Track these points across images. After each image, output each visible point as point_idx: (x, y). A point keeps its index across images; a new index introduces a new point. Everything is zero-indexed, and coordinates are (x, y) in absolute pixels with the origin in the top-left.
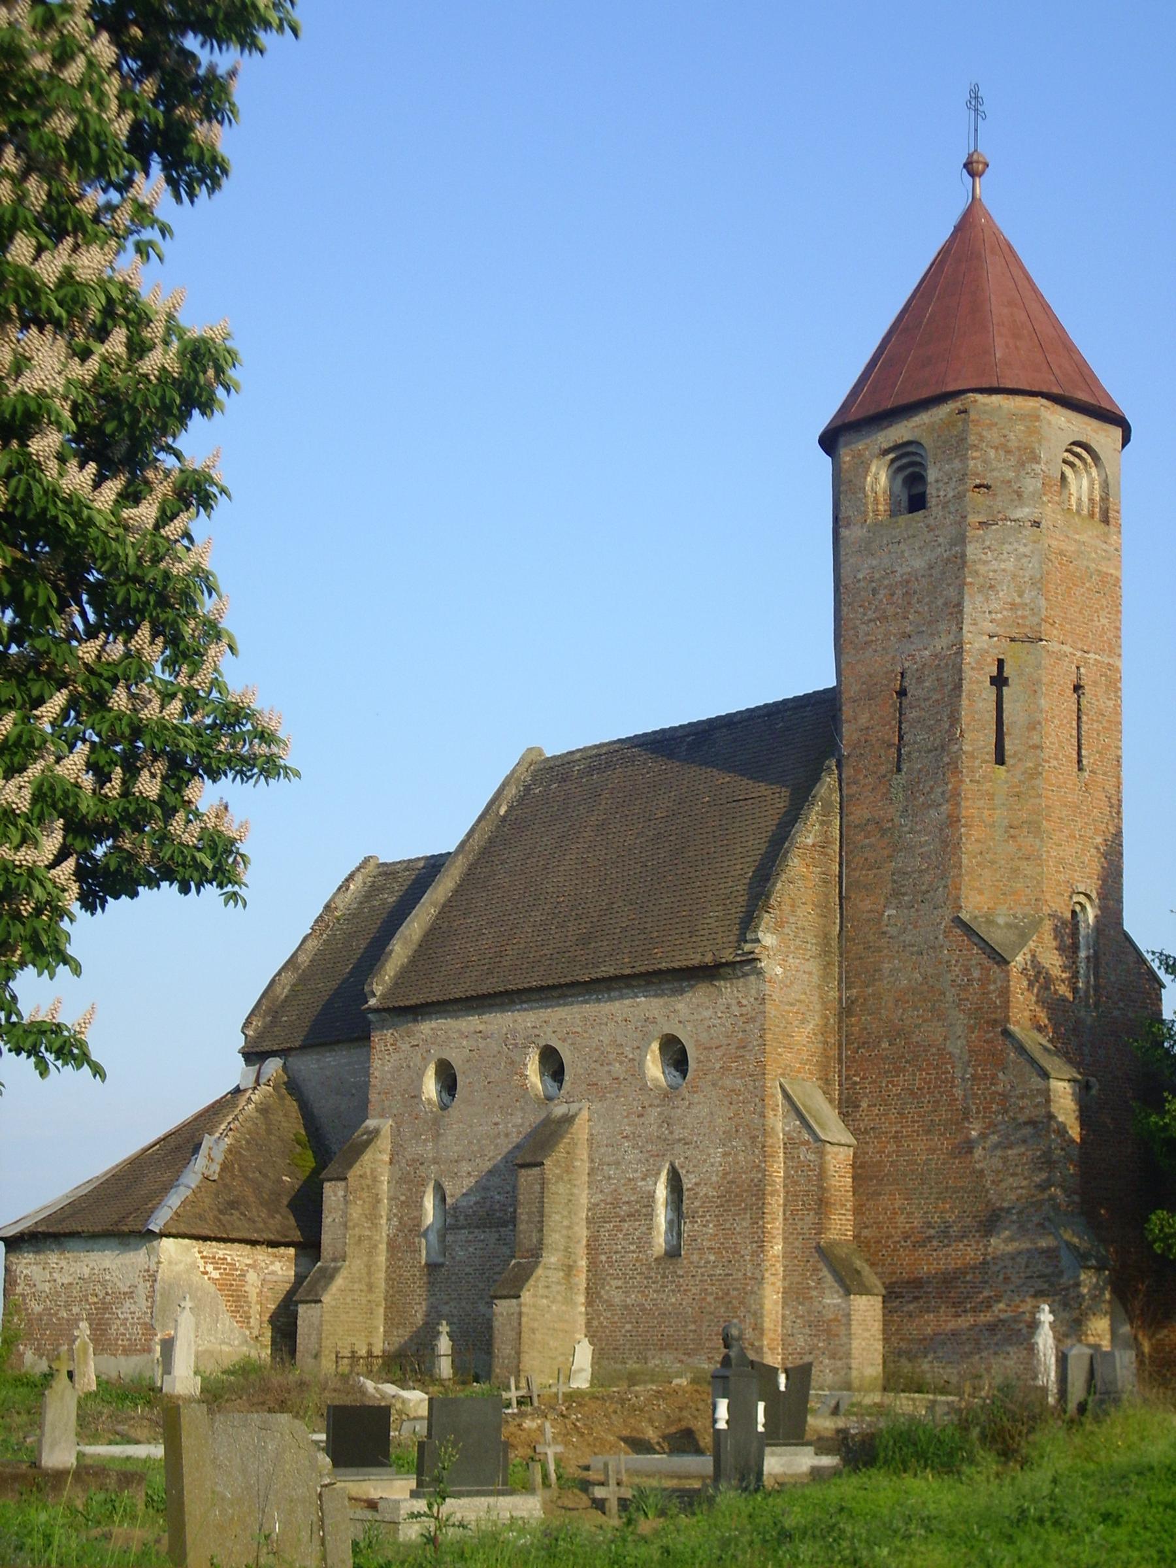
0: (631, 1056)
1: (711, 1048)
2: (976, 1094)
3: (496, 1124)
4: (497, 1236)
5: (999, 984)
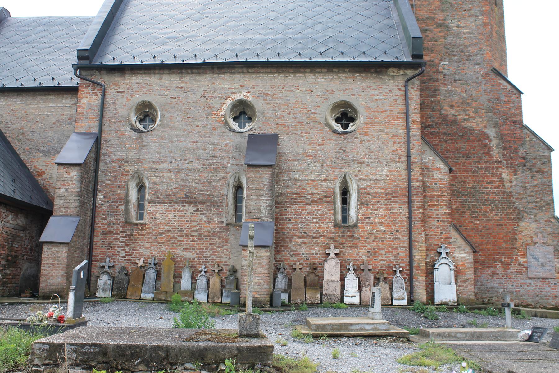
0: (313, 111)
1: (379, 112)
2: (506, 155)
3: (197, 142)
4: (195, 209)
5: (516, 104)
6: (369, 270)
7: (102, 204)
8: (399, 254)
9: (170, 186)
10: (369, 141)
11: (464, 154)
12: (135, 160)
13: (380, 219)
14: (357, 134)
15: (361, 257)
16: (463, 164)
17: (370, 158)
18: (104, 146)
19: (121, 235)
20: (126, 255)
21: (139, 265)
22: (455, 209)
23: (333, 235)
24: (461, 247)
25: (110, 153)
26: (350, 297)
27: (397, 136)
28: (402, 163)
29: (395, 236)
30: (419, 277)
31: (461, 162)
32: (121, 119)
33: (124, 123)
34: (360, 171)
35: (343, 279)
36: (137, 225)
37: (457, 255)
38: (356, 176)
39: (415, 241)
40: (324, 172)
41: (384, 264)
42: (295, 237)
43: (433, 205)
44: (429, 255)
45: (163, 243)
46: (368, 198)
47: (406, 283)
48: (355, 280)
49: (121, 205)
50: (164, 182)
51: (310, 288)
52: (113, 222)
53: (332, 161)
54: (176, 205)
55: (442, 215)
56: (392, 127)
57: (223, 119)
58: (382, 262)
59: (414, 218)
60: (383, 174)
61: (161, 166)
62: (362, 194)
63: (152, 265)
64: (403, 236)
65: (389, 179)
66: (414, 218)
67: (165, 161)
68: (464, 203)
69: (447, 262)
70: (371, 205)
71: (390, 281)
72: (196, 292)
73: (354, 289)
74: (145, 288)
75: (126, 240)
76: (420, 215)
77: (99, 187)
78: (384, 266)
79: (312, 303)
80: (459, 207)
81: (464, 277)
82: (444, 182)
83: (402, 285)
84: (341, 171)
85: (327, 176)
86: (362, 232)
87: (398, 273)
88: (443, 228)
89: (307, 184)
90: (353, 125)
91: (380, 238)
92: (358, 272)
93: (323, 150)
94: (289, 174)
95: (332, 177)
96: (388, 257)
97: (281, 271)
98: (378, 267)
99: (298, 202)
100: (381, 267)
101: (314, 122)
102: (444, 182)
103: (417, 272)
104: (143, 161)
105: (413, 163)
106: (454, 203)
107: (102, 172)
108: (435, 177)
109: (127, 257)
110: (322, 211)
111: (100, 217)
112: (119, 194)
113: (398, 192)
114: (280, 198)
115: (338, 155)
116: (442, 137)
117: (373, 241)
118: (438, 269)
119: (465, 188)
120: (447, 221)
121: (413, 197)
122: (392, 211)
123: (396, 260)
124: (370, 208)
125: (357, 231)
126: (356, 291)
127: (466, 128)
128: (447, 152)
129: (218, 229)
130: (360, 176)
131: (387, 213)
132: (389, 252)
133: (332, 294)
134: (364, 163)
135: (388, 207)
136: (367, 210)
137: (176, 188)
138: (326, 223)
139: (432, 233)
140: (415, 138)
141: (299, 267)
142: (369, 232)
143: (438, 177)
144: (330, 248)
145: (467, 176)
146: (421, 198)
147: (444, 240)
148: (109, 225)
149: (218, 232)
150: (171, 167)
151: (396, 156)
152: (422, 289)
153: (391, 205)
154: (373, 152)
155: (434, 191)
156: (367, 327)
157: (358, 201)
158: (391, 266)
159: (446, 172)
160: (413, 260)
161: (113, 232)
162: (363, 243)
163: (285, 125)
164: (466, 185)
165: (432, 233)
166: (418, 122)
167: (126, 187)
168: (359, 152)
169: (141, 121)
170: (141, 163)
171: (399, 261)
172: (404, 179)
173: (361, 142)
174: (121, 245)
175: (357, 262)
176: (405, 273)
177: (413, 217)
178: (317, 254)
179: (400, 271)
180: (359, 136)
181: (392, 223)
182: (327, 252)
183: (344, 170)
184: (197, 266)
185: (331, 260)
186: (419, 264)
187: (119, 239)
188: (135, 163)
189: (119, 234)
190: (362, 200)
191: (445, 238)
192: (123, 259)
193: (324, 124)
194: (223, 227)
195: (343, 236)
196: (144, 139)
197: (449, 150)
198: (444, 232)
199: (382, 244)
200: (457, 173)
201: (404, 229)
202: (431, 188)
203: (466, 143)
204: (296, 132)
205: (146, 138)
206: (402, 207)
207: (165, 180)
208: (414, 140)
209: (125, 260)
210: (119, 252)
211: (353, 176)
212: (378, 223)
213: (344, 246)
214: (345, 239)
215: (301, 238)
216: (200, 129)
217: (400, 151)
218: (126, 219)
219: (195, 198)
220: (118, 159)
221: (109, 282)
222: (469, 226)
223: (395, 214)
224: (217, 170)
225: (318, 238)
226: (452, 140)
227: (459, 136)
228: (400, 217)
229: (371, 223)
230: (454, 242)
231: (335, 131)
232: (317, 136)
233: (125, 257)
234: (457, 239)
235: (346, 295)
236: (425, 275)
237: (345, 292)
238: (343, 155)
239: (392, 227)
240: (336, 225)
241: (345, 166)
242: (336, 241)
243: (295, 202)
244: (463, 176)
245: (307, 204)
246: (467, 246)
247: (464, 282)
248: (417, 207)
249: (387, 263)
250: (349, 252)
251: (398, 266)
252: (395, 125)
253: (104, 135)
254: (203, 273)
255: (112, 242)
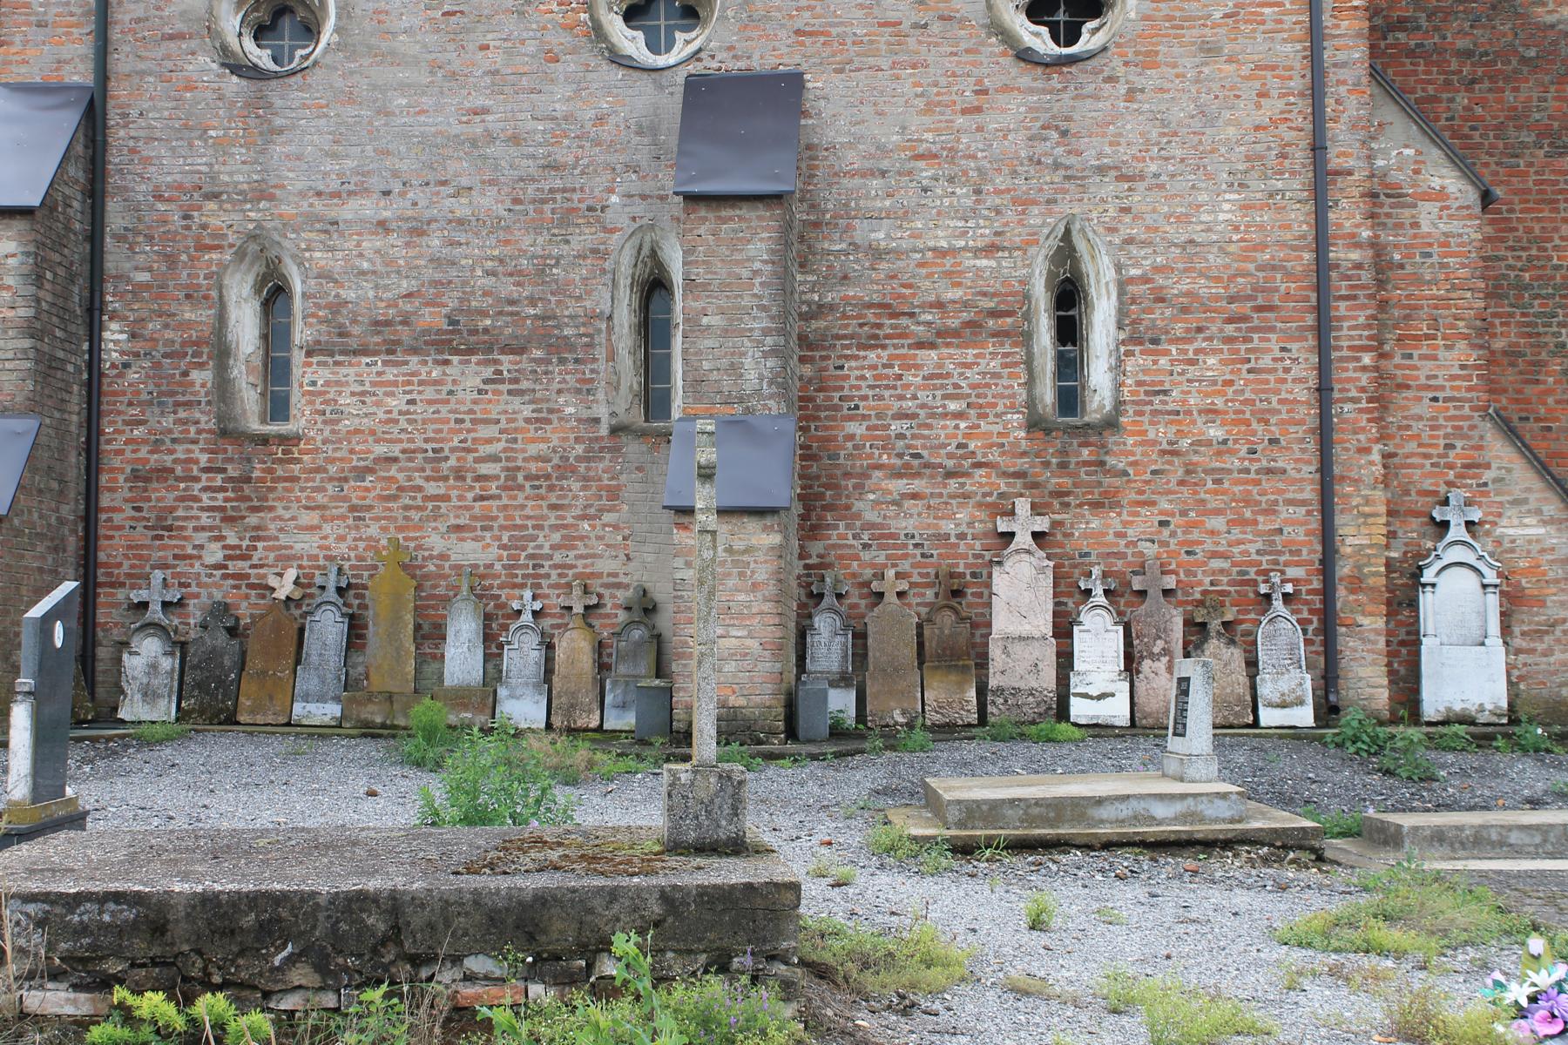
3: (485, 111)
4: (488, 372)
6: (1167, 593)
7: (126, 365)
8: (1280, 531)
9: (386, 288)
10: (1162, 90)
11: (1544, 133)
12: (245, 186)
13: (1207, 395)
14: (1115, 64)
15: (1134, 544)
16: (1537, 173)
17: (1167, 159)
18: (119, 136)
19: (203, 483)
20: (227, 557)
21: (281, 594)
22: (1505, 353)
23: (1022, 463)
24: (1525, 501)
25: (147, 161)
26: (1092, 698)
27: (1273, 68)
28: (1293, 173)
29: (1264, 463)
30: (1361, 619)
31: (1531, 164)
32: (180, 26)
33: (193, 44)
34: (1126, 210)
35: (1063, 629)
36: (264, 440)
37: (1511, 531)
38: (1112, 230)
39: (1343, 478)
40: (986, 218)
41: (1222, 571)
42: (877, 474)
43: (1415, 338)
44: (1400, 534)
45: (370, 508)
46: (1161, 314)
47: (1307, 642)
48: (1112, 635)
49: (201, 366)
50: (363, 273)
51: (937, 668)
52: (170, 431)
53: (1014, 174)
54: (414, 359)
55: (1453, 378)
56: (1254, 30)
57: (583, 16)
58: (1216, 564)
59: (1341, 390)
60: (1216, 222)
61: (349, 210)
62: (1133, 301)
63: (331, 594)
64: (1297, 461)
65: (1242, 240)
66: (1341, 390)
67: (363, 191)
68: (1541, 330)
69: (1470, 558)
70: (1171, 341)
71: (1249, 633)
72: (502, 692)
73: (1109, 667)
74: (307, 680)
75: (226, 500)
76: (1364, 379)
77: (109, 298)
78: (1225, 579)
79: (947, 724)
80: (1517, 344)
81: (1538, 614)
82: (1459, 245)
83: (1293, 648)
84: (1050, 213)
85: (997, 234)
86: (1139, 450)
87: (1278, 604)
88: (1454, 427)
89: (921, 265)
90: (1097, 29)
91: (1206, 472)
92: (1122, 601)
93: (980, 129)
94: (849, 227)
95: (1016, 236)
96: (1240, 542)
97: (824, 604)
98: (1200, 583)
99: (887, 337)
100: (1212, 584)
101: (942, 18)
102: (1459, 245)
103: (1352, 597)
104: (278, 192)
105: (1337, 173)
106: (1499, 330)
107: (120, 238)
108: (1425, 228)
109: (234, 567)
110: (981, 368)
111: (119, 413)
112: (188, 325)
113: (1277, 290)
114: (814, 324)
115: (1041, 148)
116: (1454, 66)
117: (1181, 483)
118: (1433, 585)
119: (1544, 268)
120: (1471, 400)
121: (1337, 308)
122: (1252, 364)
123: (1270, 553)
124: (1167, 353)
125: (1116, 443)
126: (1114, 676)
127: (1552, 26)
128: (1473, 128)
129: (580, 449)
130: (1125, 231)
131: (1232, 372)
132: (1243, 522)
133: (1022, 685)
134: (1142, 178)
135: (1238, 351)
136: (1155, 362)
137: (409, 295)
138: (997, 415)
139: (1412, 446)
140: (1343, 74)
141: (894, 585)
142: (1165, 446)
143: (1435, 225)
144: (1012, 513)
145: (1552, 220)
146: (1369, 312)
147: (1461, 476)
148: (156, 446)
149: (578, 459)
150: (387, 214)
151: (1269, 148)
152: (1374, 663)
153: (1251, 340)
154: (1175, 134)
155: (1418, 280)
156: (1160, 810)
157: (1120, 327)
158: (1253, 576)
159: (1468, 207)
160: (1337, 552)
161: (172, 471)
162: (1140, 492)
163: (828, 34)
164: (1550, 258)
165: (1412, 446)
166: (1356, 8)
167: (214, 294)
168: (1120, 135)
169: (261, 33)
170: (271, 198)
171: (1282, 559)
172: (1303, 237)
173: (1131, 95)
174: (205, 518)
175: (1119, 565)
176: (1306, 602)
177: (1337, 386)
178: (961, 536)
179: (1285, 595)
180: (1121, 71)
181: (1253, 413)
182: (1003, 526)
183: (1064, 208)
184: (504, 593)
185: (1017, 557)
186: (1359, 567)
187: (196, 499)
188: (245, 201)
189: (197, 479)
190: (1133, 322)
191: (1465, 466)
192: (218, 573)
193: (983, 26)
194: (597, 439)
195: (1063, 465)
196: (278, 103)
197: (1481, 119)
198: (1459, 444)
199: (1216, 492)
200: (1511, 211)
201: (1300, 435)
202: (1409, 269)
203: (1552, 88)
204: (871, 61)
205: (287, 98)
206: (1294, 346)
207: (365, 265)
208: (1340, 82)
209: (225, 577)
210: (201, 547)
211: (1101, 230)
212: (1200, 412)
213: (1067, 505)
214: (1070, 475)
215: (899, 476)
216: (496, 58)
217: (1283, 127)
218: (220, 419)
219: (486, 331)
220: (179, 187)
221: (166, 664)
222: (1557, 419)
223: (1264, 376)
224: (566, 218)
225: (967, 475)
226: (1493, 79)
227: (1524, 60)
228: (1284, 387)
229: (1169, 413)
230: (1496, 480)
231: (1025, 56)
232: (954, 75)
233: (226, 567)
234: (1509, 470)
235: (1078, 690)
236: (1383, 608)
237: (1074, 680)
238: (1060, 150)
239: (1255, 425)
240: (1035, 424)
241: (1066, 192)
242: (1035, 485)
243: (876, 337)
244: (1539, 220)
245: (920, 345)
246: (1549, 495)
247: (1539, 634)
248: (1351, 348)
249: (1234, 564)
250: (1088, 527)
251: (1276, 579)
252: (1263, 22)
253: (119, 91)
254: (527, 618)
255: (172, 509)
